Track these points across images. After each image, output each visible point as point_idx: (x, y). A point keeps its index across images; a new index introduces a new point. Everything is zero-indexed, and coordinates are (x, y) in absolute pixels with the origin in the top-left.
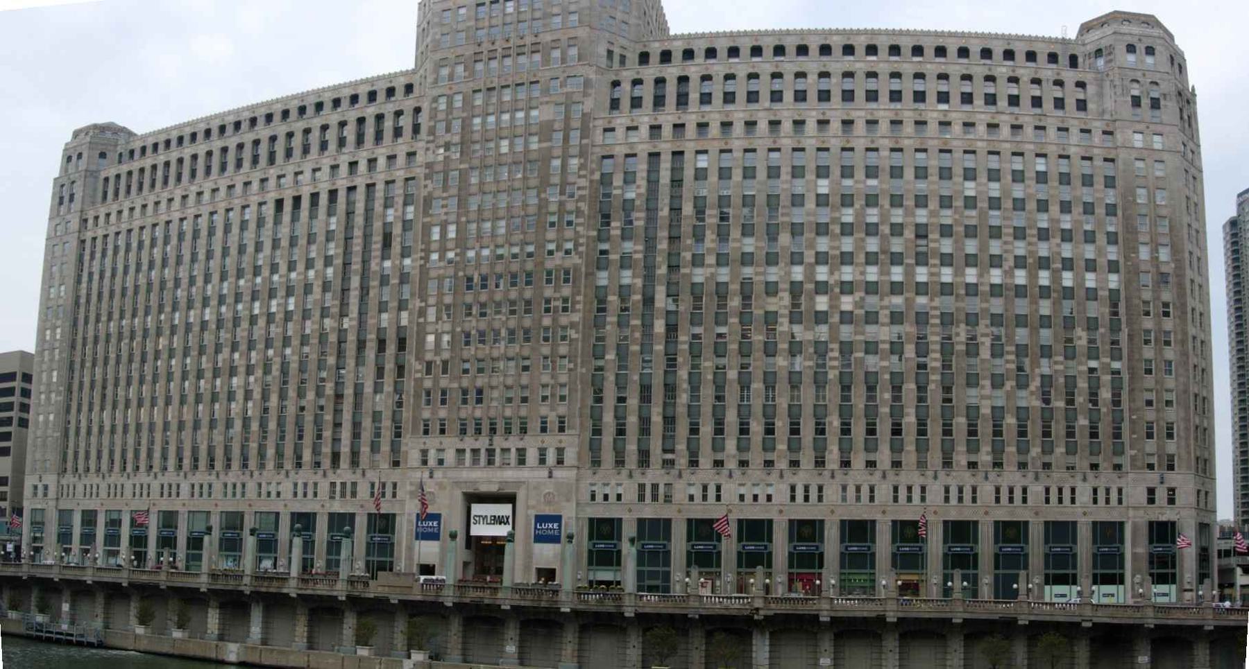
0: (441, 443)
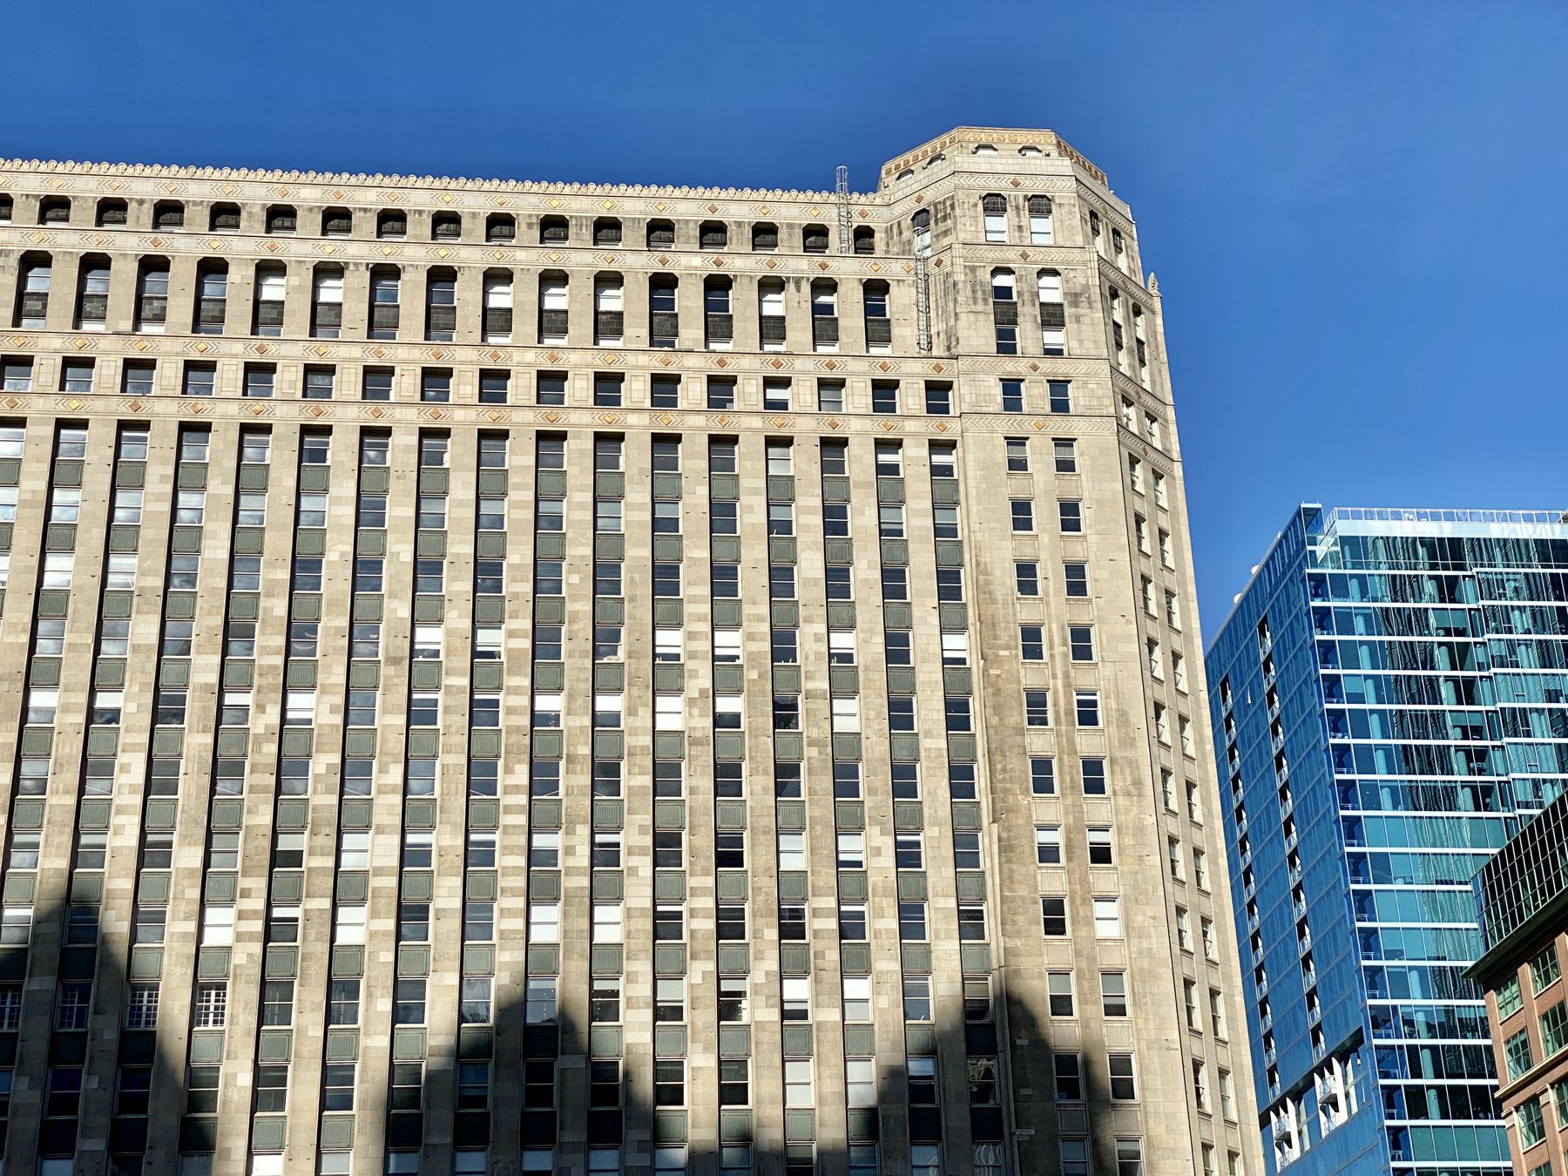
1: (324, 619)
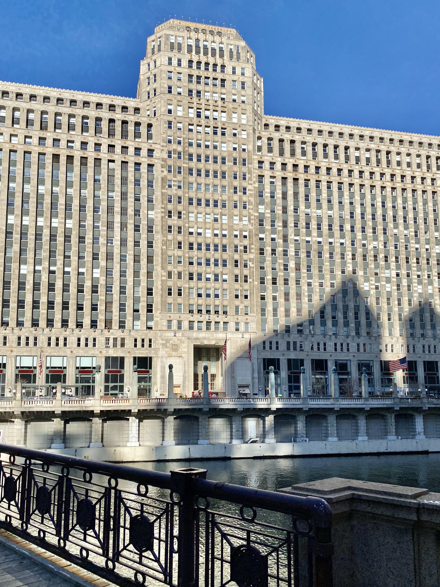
0: (180, 317)
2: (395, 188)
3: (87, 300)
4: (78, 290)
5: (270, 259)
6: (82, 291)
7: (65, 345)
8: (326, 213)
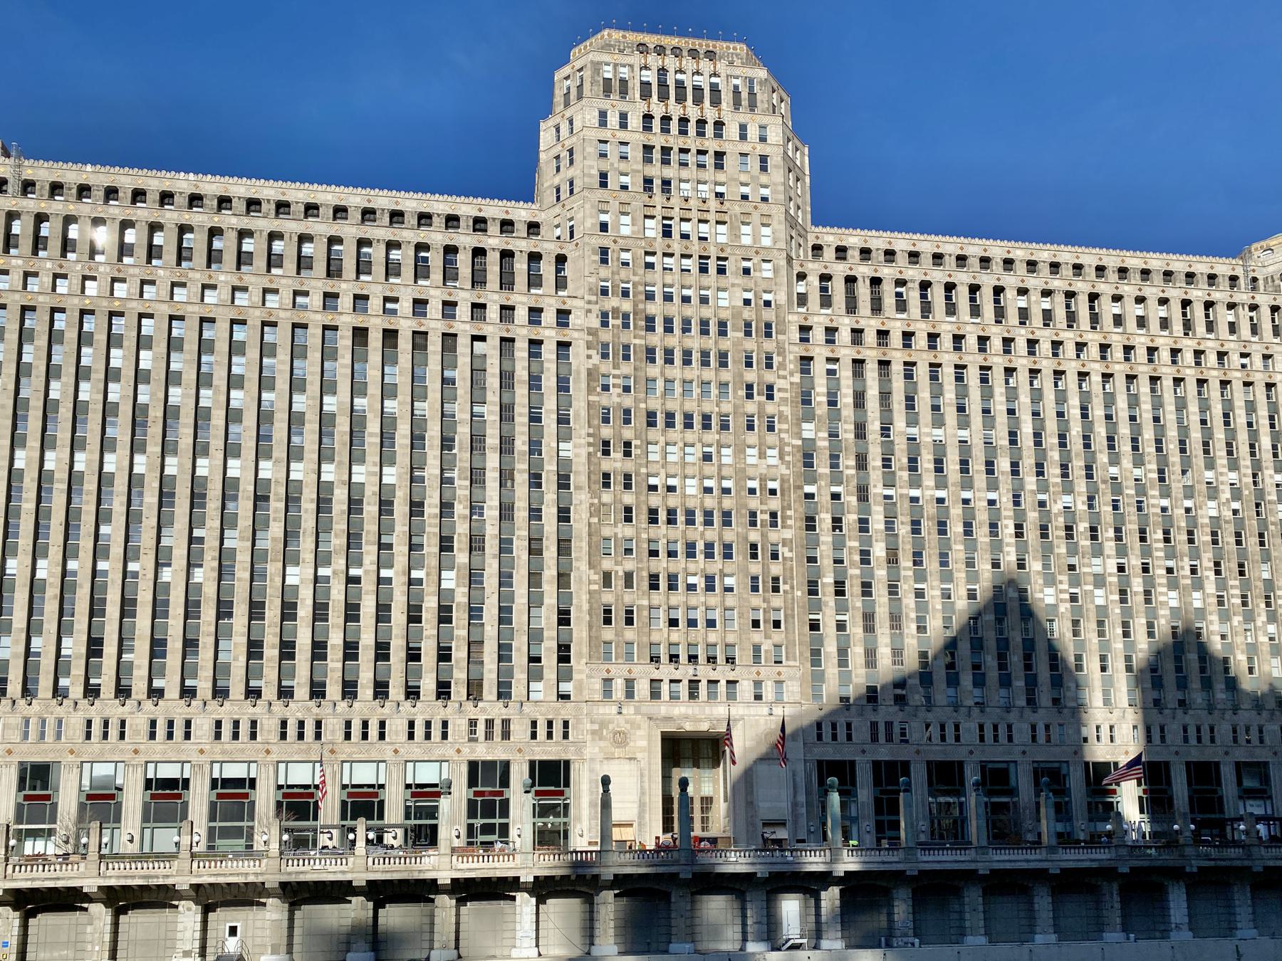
1: (1074, 462)
2: (1111, 375)
3: (428, 637)
4: (409, 616)
5: (830, 539)
6: (418, 620)
7: (382, 736)
8: (955, 435)
